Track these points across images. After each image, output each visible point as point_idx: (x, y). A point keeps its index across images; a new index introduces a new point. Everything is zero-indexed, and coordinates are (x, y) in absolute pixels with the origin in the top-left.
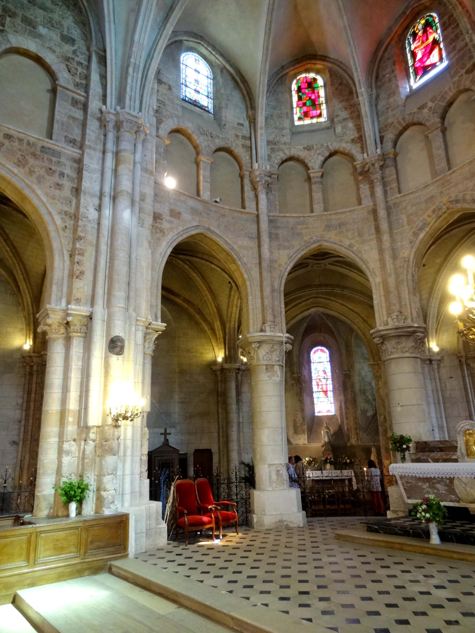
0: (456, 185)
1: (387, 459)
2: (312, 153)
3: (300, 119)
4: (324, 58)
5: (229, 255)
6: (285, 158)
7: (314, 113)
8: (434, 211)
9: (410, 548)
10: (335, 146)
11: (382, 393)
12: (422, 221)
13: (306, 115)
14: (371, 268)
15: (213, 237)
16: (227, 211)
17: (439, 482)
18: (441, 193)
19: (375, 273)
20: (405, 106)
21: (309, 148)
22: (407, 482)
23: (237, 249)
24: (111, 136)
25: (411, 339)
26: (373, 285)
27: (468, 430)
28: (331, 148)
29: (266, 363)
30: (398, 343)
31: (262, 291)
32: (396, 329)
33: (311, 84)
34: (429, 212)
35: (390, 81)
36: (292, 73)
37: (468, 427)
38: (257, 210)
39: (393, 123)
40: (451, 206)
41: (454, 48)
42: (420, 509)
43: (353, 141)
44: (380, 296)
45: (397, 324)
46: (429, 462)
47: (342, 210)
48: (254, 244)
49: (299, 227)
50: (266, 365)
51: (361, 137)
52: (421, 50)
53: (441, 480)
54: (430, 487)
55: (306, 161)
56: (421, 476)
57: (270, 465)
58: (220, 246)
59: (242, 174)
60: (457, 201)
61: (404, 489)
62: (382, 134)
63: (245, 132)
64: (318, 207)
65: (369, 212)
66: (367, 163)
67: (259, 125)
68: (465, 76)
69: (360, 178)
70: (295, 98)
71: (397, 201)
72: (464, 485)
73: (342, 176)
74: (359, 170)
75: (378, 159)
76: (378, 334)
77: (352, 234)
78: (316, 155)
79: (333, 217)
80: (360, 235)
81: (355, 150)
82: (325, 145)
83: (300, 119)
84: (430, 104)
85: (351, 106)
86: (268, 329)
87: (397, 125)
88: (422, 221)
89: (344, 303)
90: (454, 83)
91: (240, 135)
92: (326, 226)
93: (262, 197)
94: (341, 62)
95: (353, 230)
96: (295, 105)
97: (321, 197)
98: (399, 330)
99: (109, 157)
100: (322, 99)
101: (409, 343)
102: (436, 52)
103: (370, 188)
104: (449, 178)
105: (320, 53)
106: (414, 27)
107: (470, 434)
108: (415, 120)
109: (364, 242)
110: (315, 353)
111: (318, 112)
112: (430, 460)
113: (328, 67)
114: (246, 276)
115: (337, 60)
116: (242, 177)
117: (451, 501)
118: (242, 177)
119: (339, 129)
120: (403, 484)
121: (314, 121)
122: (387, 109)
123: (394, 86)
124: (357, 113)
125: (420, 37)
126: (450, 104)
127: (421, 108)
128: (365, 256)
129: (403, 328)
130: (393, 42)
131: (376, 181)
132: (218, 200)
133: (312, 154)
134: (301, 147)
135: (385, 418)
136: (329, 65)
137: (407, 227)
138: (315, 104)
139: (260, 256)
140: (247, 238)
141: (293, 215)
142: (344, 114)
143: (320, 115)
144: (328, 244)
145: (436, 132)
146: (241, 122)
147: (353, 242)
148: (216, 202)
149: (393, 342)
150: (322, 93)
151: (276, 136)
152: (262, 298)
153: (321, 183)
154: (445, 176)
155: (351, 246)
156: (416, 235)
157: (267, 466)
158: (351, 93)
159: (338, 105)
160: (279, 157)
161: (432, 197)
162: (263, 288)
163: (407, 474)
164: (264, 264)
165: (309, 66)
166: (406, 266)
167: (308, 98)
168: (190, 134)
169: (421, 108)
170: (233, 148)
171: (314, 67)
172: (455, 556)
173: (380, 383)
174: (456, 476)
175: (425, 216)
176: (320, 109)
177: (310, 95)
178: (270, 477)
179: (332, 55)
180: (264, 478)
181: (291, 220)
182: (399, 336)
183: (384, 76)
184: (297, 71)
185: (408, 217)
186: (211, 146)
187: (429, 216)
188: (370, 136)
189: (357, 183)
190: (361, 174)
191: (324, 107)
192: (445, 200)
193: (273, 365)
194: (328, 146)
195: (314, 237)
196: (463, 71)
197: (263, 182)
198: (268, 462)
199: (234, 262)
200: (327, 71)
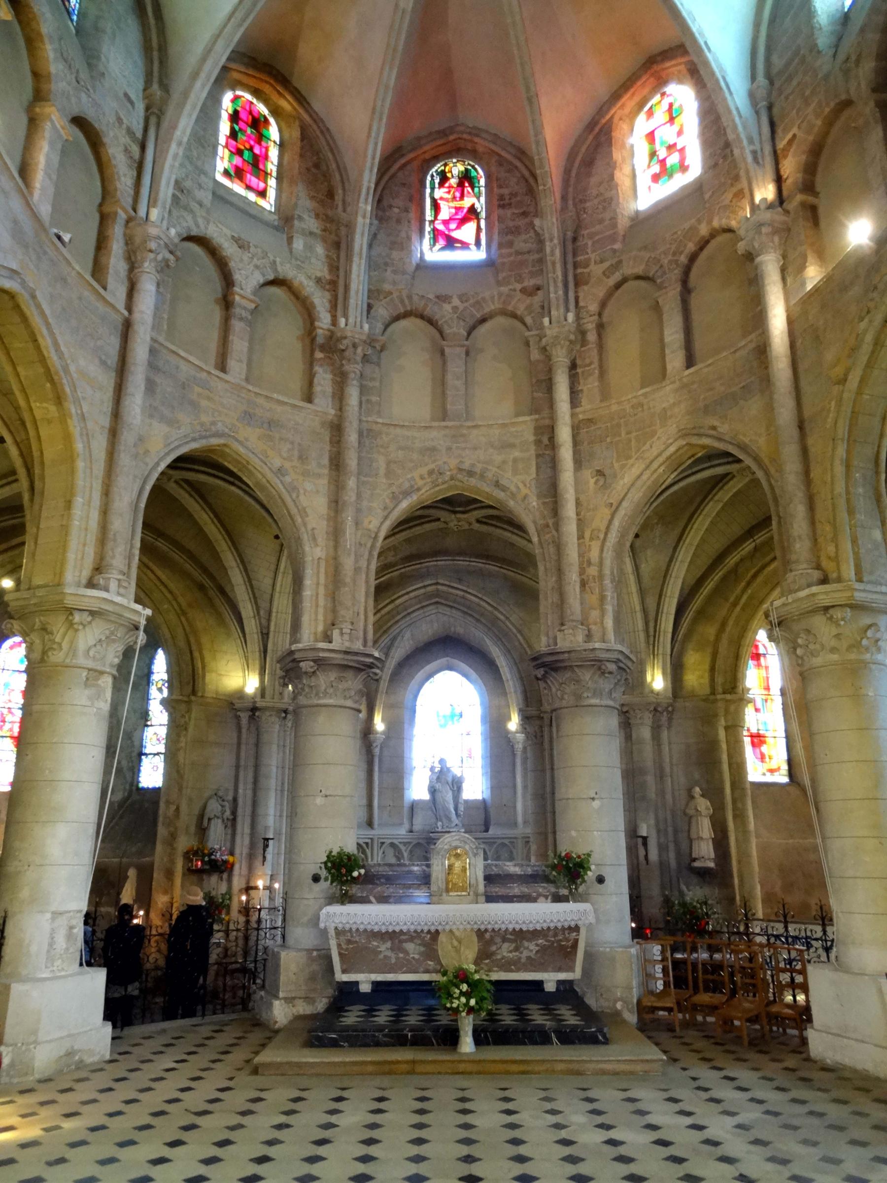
0: (475, 449)
1: (165, 892)
2: (246, 257)
3: (226, 173)
4: (300, 98)
5: (52, 381)
6: (193, 233)
8: (431, 473)
9: (429, 1068)
10: (287, 270)
11: (182, 761)
12: (409, 480)
13: (238, 173)
14: (309, 527)
15: (36, 320)
16: (74, 273)
17: (411, 939)
18: (449, 449)
19: (314, 539)
20: (413, 278)
21: (242, 245)
22: (349, 942)
23: (75, 375)
25: (362, 676)
26: (308, 559)
27: (456, 848)
28: (279, 269)
29: (90, 664)
30: (340, 679)
31: (107, 493)
32: (346, 653)
33: (258, 123)
34: (424, 471)
35: (399, 221)
36: (236, 75)
37: (457, 843)
38: (129, 307)
39: (390, 293)
40: (459, 476)
41: (510, 244)
42: (457, 991)
43: (318, 281)
44: (318, 584)
45: (347, 644)
46: (370, 902)
47: (281, 398)
48: (108, 381)
49: (197, 389)
50: (90, 670)
51: (333, 284)
52: (450, 208)
53: (415, 936)
54: (392, 949)
55: (232, 264)
56: (376, 929)
57: (56, 914)
58: (38, 348)
59: (107, 209)
60: (471, 473)
61: (340, 954)
62: (371, 301)
63: (135, 123)
64: (237, 368)
65: (323, 424)
66: (345, 338)
67: (178, 133)
68: (519, 295)
69: (319, 355)
70: (225, 127)
71: (374, 427)
72: (456, 943)
73: (284, 332)
74: (320, 340)
75: (365, 342)
76: (311, 655)
77: (289, 450)
78: (251, 267)
79: (260, 401)
81: (320, 301)
82: (272, 258)
83: (226, 173)
84: (456, 302)
85: (327, 216)
86: (113, 585)
87: (397, 301)
88: (409, 480)
89: (151, 564)
90: (500, 295)
91: (125, 121)
92: (245, 412)
93: (148, 289)
94: (328, 129)
95: (292, 443)
96: (222, 140)
97: (245, 350)
98: (349, 657)
100: (272, 166)
101: (354, 683)
102: (471, 227)
103: (334, 382)
104: (465, 432)
105: (296, 83)
106: (445, 165)
107: (457, 856)
108: (428, 312)
109: (306, 474)
110: (11, 648)
111: (262, 185)
112: (372, 899)
113: (301, 121)
114: (79, 446)
115: (322, 120)
116: (105, 219)
117: (427, 971)
118: (105, 219)
119: (299, 244)
120: (339, 945)
121: (252, 197)
122: (386, 264)
123: (403, 234)
124: (333, 237)
125: (450, 187)
126: (483, 320)
127: (443, 298)
128: (304, 501)
129: (356, 654)
130: (416, 164)
131: (352, 375)
132: (66, 237)
133: (245, 258)
134: (229, 233)
135: (178, 809)
136: (306, 116)
137: (384, 481)
138: (257, 163)
139: (116, 414)
140: (97, 361)
141: (191, 358)
142: (312, 224)
143: (262, 194)
144: (241, 450)
145: (458, 350)
146: (133, 97)
147: (287, 465)
148: (59, 238)
149: (333, 675)
150: (274, 153)
151: (187, 176)
152: (105, 511)
153: (250, 324)
154: (461, 426)
155: (281, 472)
156: (396, 499)
157: (48, 916)
158: (331, 195)
159: (304, 203)
160: (185, 224)
161: (433, 449)
162: (115, 490)
163: (354, 927)
164: (127, 437)
165: (267, 89)
166: (369, 545)
167: (247, 146)
168: (39, 34)
169: (443, 298)
170: (106, 140)
171: (274, 97)
172: (514, 1068)
173: (182, 739)
174: (440, 928)
175: (416, 474)
176: (265, 182)
177: (252, 143)
178: (51, 945)
179: (317, 106)
180: (34, 949)
181: (184, 366)
182: (345, 667)
183: (391, 207)
184: (245, 79)
185: (388, 463)
186: (73, 100)
187: (422, 478)
188: (357, 292)
189: (310, 363)
190: (322, 348)
191: (272, 182)
192: (453, 463)
193: (102, 673)
194: (275, 262)
195: (220, 424)
196: (518, 286)
197: (160, 257)
198: (53, 908)
199: (59, 400)
200: (297, 123)
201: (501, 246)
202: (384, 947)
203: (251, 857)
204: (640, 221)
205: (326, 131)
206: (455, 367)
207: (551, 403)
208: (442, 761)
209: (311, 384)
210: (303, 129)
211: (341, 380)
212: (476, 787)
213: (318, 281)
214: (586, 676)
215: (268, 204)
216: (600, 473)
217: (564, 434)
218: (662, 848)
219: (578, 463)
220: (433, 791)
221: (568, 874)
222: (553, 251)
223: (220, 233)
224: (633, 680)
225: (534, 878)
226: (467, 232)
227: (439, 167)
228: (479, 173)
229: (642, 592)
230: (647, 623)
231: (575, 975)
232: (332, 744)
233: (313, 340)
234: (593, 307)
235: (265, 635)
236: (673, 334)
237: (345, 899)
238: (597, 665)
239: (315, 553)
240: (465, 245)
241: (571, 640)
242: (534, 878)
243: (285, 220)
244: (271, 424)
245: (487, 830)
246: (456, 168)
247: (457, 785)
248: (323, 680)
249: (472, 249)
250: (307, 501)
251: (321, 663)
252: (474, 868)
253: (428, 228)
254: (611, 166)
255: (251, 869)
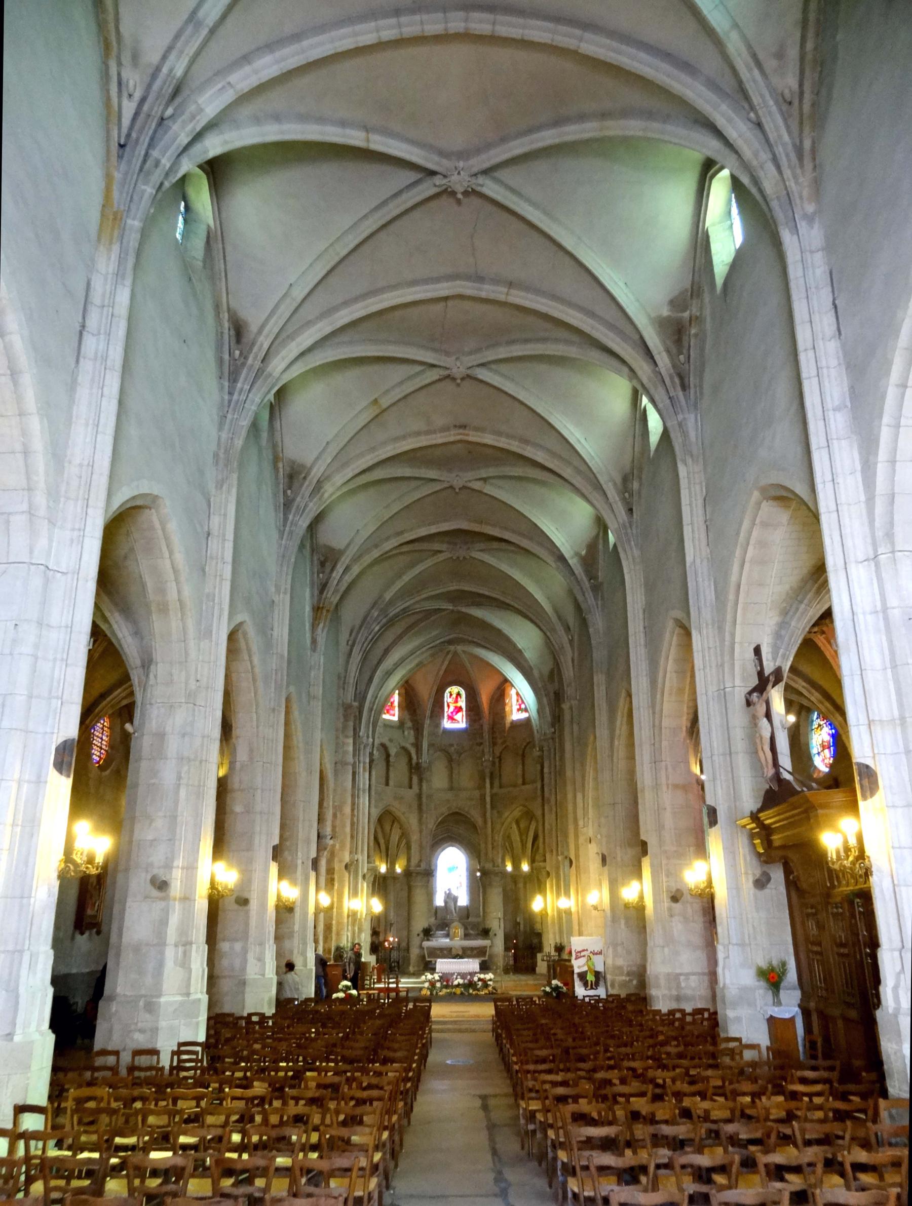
7: (392, 712)
10: (403, 744)
24: (362, 753)
43: (412, 744)
64: (391, 783)
80: (410, 806)
81: (413, 751)
99: (362, 765)
102: (460, 714)
119: (406, 733)
127: (452, 745)
142: (409, 724)
155: (404, 814)
158: (415, 711)
159: (407, 717)
169: (452, 745)
189: (411, 773)
191: (397, 709)
201: (470, 725)
202: (438, 952)
203: (386, 931)
204: (513, 722)
205: (413, 689)
206: (455, 772)
207: (485, 787)
208: (449, 890)
209: (411, 779)
210: (406, 689)
211: (421, 781)
212: (463, 901)
213: (412, 744)
214: (492, 876)
215: (396, 718)
216: (498, 812)
217: (488, 799)
218: (525, 926)
219: (492, 808)
220: (446, 902)
221: (486, 933)
222: (486, 735)
223: (385, 740)
224: (517, 866)
225: (478, 934)
226: (459, 716)
227: (449, 690)
228: (463, 693)
229: (521, 835)
230: (523, 845)
231: (486, 958)
232: (419, 896)
233: (411, 764)
234: (498, 754)
235: (387, 849)
236: (519, 771)
237: (428, 940)
238: (496, 874)
239: (415, 837)
240: (458, 722)
241: (488, 866)
242: (478, 934)
243: (401, 723)
244: (402, 798)
245: (468, 918)
246: (455, 689)
247: (455, 899)
248: (419, 878)
249: (460, 722)
250: (412, 821)
251: (418, 873)
252: (460, 932)
253: (446, 715)
254: (504, 704)
255: (386, 934)
